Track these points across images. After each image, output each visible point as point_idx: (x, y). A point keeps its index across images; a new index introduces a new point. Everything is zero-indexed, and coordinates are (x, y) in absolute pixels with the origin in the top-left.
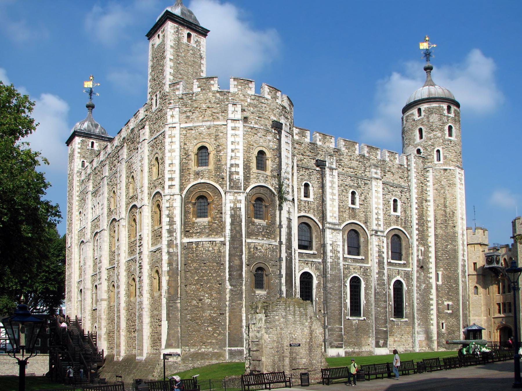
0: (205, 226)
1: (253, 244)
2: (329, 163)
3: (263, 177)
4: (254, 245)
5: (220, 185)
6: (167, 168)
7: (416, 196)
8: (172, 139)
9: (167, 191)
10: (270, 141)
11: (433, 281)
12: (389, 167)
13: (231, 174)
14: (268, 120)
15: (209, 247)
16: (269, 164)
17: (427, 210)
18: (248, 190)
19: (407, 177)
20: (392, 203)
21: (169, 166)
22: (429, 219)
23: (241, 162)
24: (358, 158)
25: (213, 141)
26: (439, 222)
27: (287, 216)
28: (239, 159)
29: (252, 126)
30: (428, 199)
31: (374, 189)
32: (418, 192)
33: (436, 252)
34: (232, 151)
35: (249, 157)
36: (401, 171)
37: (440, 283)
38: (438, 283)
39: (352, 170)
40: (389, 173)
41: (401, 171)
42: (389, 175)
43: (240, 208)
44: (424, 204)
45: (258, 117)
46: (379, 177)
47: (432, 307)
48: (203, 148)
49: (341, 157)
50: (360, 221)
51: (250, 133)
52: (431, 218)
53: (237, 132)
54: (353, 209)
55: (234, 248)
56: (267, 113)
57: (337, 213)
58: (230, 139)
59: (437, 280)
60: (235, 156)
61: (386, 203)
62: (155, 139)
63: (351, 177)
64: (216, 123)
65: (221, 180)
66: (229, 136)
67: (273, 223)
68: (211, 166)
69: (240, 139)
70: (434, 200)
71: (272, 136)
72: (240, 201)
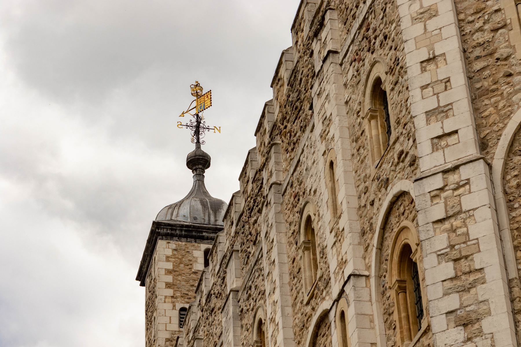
21: (423, 70)
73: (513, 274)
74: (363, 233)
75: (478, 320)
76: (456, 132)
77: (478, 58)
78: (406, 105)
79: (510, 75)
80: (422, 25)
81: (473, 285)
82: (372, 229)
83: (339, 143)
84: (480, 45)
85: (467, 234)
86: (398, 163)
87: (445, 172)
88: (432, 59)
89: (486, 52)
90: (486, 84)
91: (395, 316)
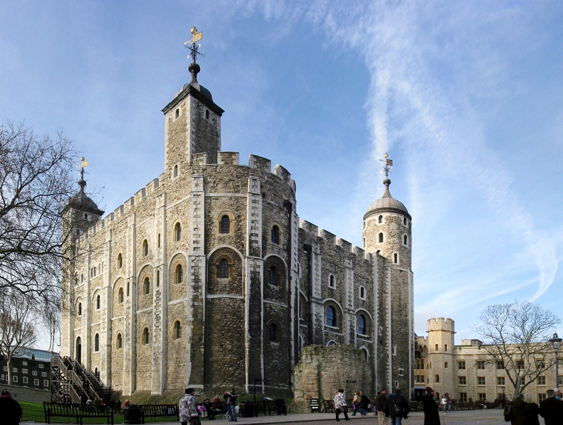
0: (225, 285)
1: (269, 304)
2: (314, 249)
3: (277, 249)
4: (270, 305)
5: (240, 251)
7: (378, 288)
8: (197, 206)
10: (282, 218)
11: (389, 352)
12: (358, 261)
13: (251, 242)
14: (281, 198)
15: (230, 303)
16: (282, 237)
17: (386, 300)
18: (265, 258)
22: (387, 307)
23: (260, 232)
24: (335, 248)
25: (235, 211)
26: (395, 310)
27: (295, 285)
29: (269, 201)
30: (387, 291)
31: (348, 276)
32: (379, 285)
33: (392, 332)
34: (253, 222)
35: (267, 229)
36: (366, 266)
37: (395, 354)
38: (393, 355)
39: (331, 258)
41: (366, 266)
42: (357, 267)
43: (259, 273)
44: (384, 295)
45: (274, 195)
46: (351, 267)
47: (388, 371)
48: (225, 218)
49: (323, 245)
51: (267, 208)
52: (389, 306)
53: (257, 205)
55: (254, 305)
56: (280, 192)
59: (393, 352)
60: (255, 227)
63: (330, 264)
64: (237, 195)
65: (241, 247)
67: (283, 289)
68: (232, 233)
70: (391, 293)
71: (284, 214)
72: (259, 267)
87: (196, 256)
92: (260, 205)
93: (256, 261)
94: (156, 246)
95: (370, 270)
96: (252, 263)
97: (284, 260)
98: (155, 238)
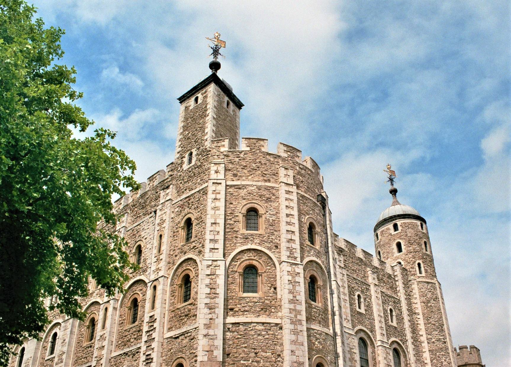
6: (209, 227)
9: (208, 255)
19: (396, 288)
20: (389, 312)
21: (212, 226)
28: (294, 226)
40: (382, 281)
50: (368, 329)
54: (360, 314)
56: (313, 185)
57: (350, 315)
58: (283, 203)
61: (385, 310)
62: (186, 198)
66: (282, 200)
69: (294, 204)
73: (226, 298)
74: (169, 263)
75: (214, 308)
76: (218, 249)
77: (228, 228)
78: (203, 233)
79: (237, 237)
80: (214, 211)
81: (215, 298)
82: (174, 264)
83: (167, 230)
84: (230, 224)
85: (216, 282)
86: (192, 249)
87: (213, 260)
88: (215, 223)
89: (231, 227)
90: (229, 237)
91: (176, 294)
92: (294, 197)
93: (294, 266)
94: (155, 251)
95: (394, 286)
96: (289, 269)
97: (323, 267)
98: (155, 241)
